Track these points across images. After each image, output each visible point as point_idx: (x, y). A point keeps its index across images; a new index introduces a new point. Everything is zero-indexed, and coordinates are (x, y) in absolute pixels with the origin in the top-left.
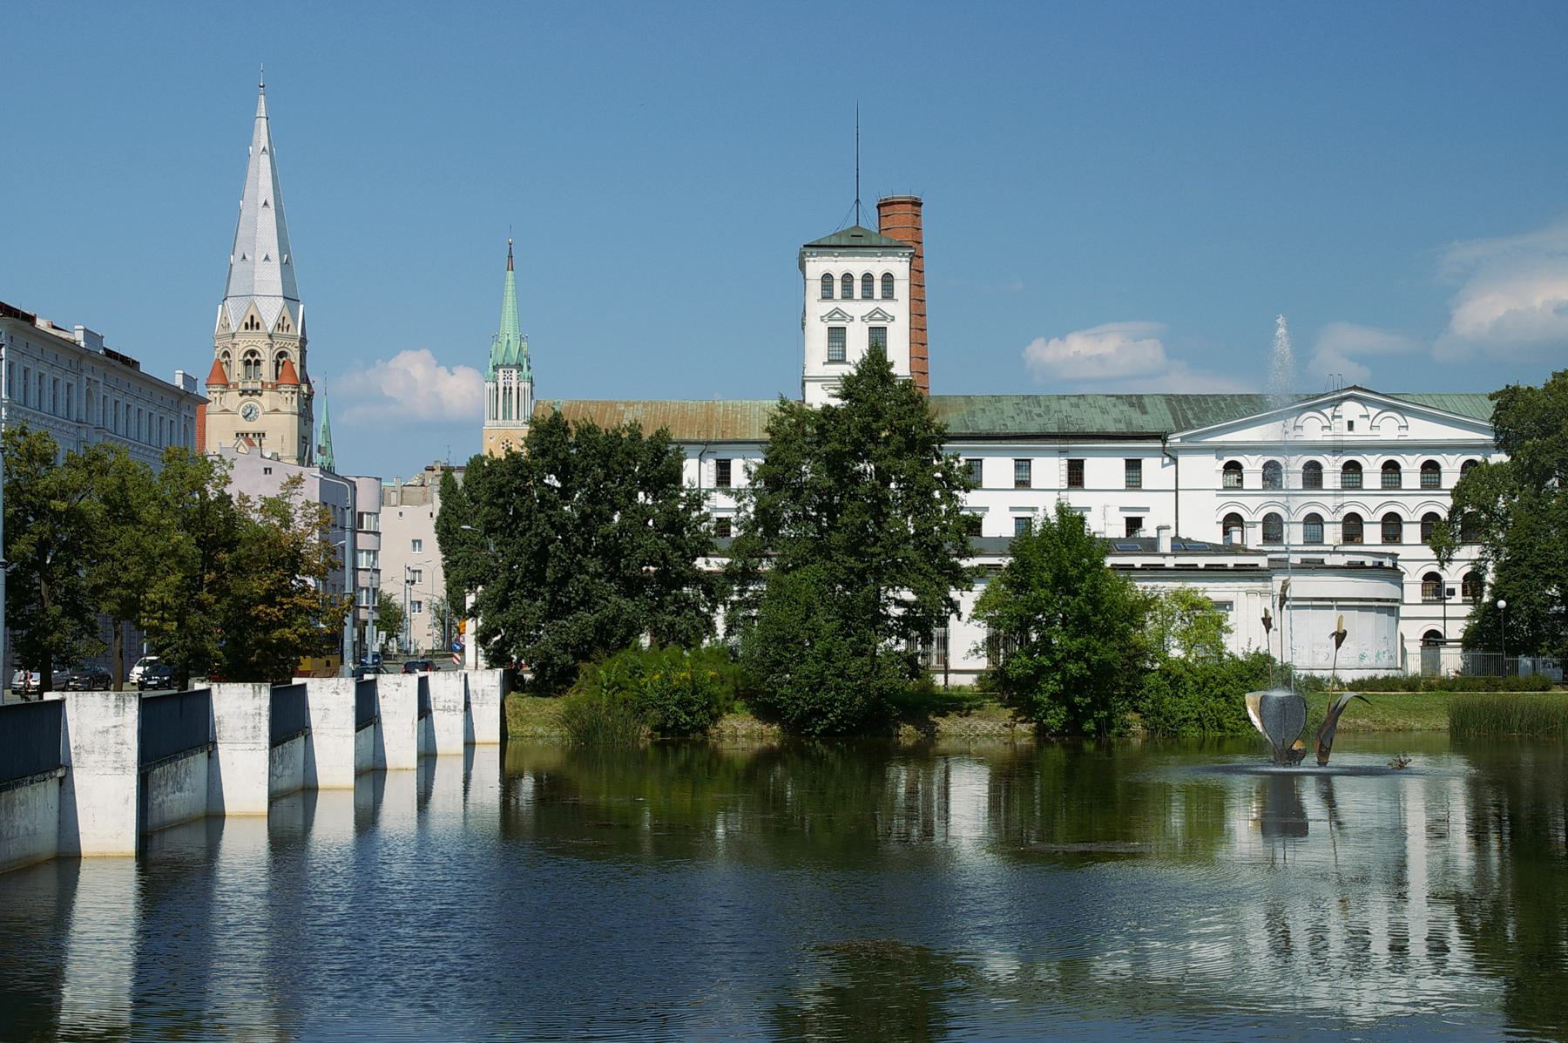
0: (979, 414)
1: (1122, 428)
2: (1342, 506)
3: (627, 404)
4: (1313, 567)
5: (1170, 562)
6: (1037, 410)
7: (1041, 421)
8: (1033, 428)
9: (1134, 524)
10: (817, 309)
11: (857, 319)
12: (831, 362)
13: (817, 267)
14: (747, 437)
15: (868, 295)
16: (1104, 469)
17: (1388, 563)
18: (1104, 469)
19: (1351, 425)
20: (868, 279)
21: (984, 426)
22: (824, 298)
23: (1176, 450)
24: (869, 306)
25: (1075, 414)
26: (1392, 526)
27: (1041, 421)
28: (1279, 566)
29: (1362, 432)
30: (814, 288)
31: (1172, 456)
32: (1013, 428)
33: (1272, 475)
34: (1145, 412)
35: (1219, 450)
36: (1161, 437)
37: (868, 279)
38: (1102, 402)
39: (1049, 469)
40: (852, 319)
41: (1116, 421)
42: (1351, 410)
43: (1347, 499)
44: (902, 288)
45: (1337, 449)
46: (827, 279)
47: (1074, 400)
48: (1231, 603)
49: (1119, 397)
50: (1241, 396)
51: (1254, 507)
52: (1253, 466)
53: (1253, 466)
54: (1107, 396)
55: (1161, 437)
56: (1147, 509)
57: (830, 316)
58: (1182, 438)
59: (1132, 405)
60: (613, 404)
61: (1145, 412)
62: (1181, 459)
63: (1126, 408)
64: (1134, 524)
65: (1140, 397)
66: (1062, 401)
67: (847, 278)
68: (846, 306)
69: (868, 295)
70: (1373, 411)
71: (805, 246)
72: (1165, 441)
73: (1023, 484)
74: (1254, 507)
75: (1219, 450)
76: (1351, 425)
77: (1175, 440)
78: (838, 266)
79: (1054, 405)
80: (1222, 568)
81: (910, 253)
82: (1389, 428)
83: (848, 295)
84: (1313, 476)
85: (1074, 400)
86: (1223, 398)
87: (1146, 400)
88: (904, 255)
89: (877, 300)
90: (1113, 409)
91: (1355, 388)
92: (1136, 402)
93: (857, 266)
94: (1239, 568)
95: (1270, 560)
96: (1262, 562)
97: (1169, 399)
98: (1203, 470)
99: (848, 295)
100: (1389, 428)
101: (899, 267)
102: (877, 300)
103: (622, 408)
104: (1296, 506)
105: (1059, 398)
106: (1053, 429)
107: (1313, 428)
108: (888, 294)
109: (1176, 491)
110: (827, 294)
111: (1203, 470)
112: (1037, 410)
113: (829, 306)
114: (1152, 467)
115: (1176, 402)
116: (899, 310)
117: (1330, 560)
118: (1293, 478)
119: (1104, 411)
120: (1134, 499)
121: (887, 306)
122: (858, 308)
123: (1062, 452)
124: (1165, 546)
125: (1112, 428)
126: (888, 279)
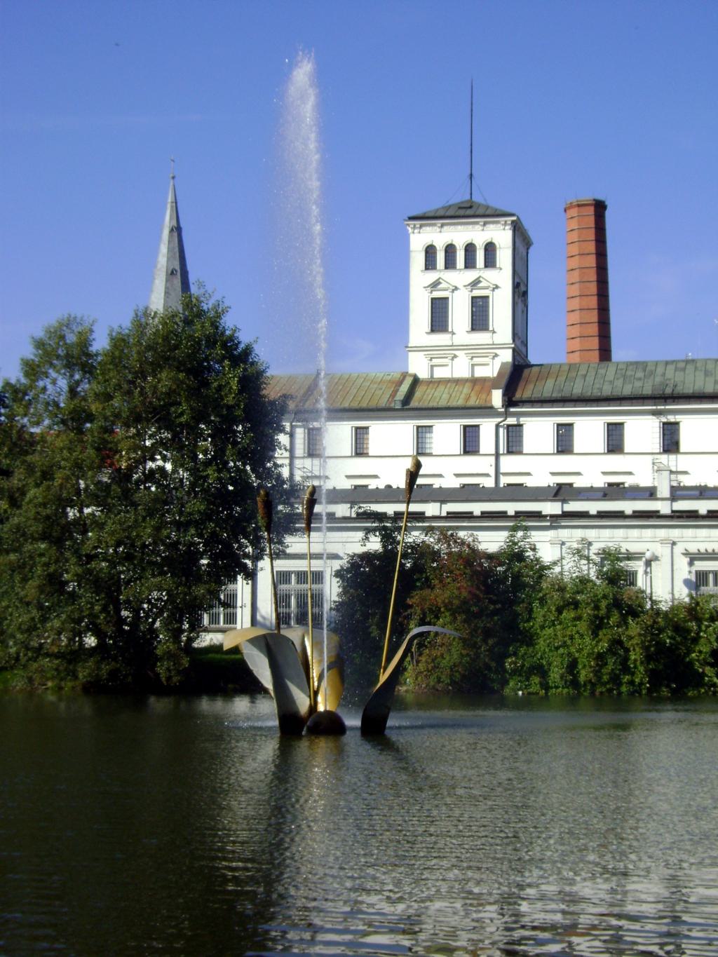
5: (664, 508)
8: (627, 391)
10: (419, 279)
13: (420, 239)
15: (470, 263)
20: (470, 249)
22: (427, 268)
24: (471, 275)
25: (679, 377)
27: (638, 384)
30: (418, 260)
32: (607, 391)
37: (470, 249)
40: (456, 288)
44: (505, 257)
46: (430, 251)
57: (435, 285)
66: (671, 368)
67: (450, 250)
68: (452, 277)
69: (470, 263)
78: (439, 236)
81: (513, 222)
83: (450, 264)
85: (682, 365)
88: (506, 224)
89: (480, 269)
93: (460, 235)
99: (450, 264)
101: (502, 236)
102: (480, 269)
105: (667, 363)
106: (648, 390)
108: (490, 262)
110: (430, 264)
113: (432, 276)
116: (502, 276)
121: (490, 276)
122: (460, 277)
124: (664, 491)
126: (490, 249)
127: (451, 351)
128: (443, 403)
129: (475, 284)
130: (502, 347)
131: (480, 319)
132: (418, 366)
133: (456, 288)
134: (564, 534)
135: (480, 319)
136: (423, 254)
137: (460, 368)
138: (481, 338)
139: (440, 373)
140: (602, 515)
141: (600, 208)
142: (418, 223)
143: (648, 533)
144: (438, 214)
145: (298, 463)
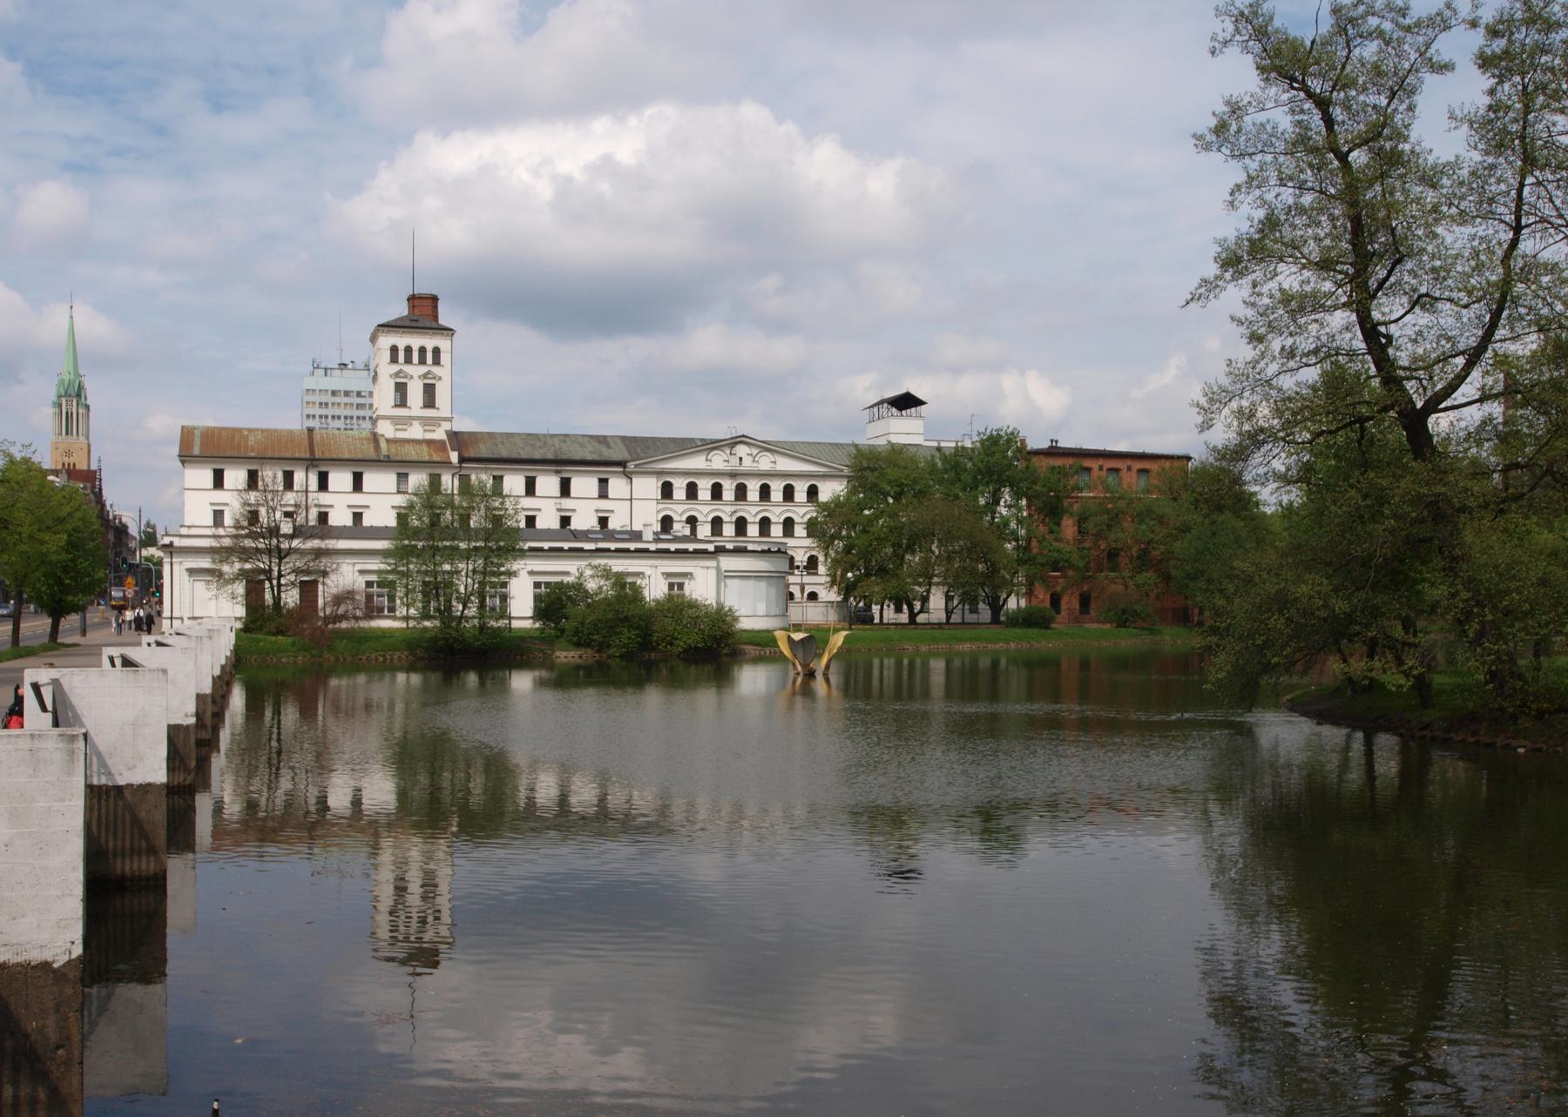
0: (500, 446)
1: (595, 457)
2: (735, 512)
3: (250, 430)
4: (740, 551)
5: (652, 547)
6: (539, 444)
7: (541, 451)
8: (537, 456)
9: (603, 521)
11: (415, 376)
12: (396, 406)
13: (386, 341)
14: (340, 456)
15: (422, 361)
16: (585, 485)
17: (783, 550)
18: (585, 485)
19: (741, 459)
21: (504, 454)
23: (632, 473)
24: (423, 369)
26: (789, 525)
28: (720, 550)
29: (747, 462)
31: (628, 476)
32: (524, 455)
33: (692, 491)
34: (608, 446)
35: (659, 473)
36: (622, 464)
38: (581, 440)
39: (548, 484)
41: (591, 452)
42: (742, 450)
43: (738, 507)
45: (733, 475)
46: (394, 349)
47: (562, 438)
48: (691, 574)
49: (591, 437)
50: (669, 439)
51: (679, 510)
52: (679, 486)
53: (679, 486)
54: (583, 436)
55: (622, 464)
56: (612, 511)
57: (397, 375)
58: (636, 466)
59: (600, 442)
60: (239, 430)
61: (608, 446)
62: (635, 480)
63: (595, 444)
64: (603, 521)
65: (605, 437)
66: (555, 439)
68: (408, 369)
69: (422, 361)
70: (755, 451)
71: (379, 326)
72: (625, 467)
73: (603, 495)
74: (679, 510)
75: (659, 473)
76: (741, 459)
77: (631, 466)
78: (402, 341)
79: (549, 440)
80: (685, 551)
82: (765, 463)
83: (408, 360)
84: (717, 492)
85: (562, 438)
86: (659, 439)
87: (609, 439)
90: (588, 445)
91: (743, 436)
92: (602, 440)
93: (416, 341)
94: (696, 552)
95: (716, 547)
96: (711, 548)
97: (624, 439)
98: (648, 487)
100: (765, 463)
103: (246, 433)
104: (705, 511)
106: (550, 456)
107: (718, 461)
108: (437, 361)
109: (631, 499)
110: (394, 360)
111: (648, 487)
112: (539, 444)
113: (395, 368)
114: (617, 485)
115: (628, 441)
117: (750, 547)
118: (704, 494)
119: (582, 446)
120: (603, 504)
121: (436, 370)
122: (416, 370)
123: (557, 472)
125: (589, 457)
126: (436, 351)
127: (408, 421)
128: (415, 458)
129: (425, 376)
130: (445, 419)
131: (430, 399)
132: (386, 429)
133: (412, 377)
134: (596, 562)
135: (430, 399)
136: (389, 352)
137: (416, 432)
138: (430, 413)
139: (401, 435)
140: (618, 550)
141: (434, 299)
142: (386, 329)
143: (643, 562)
144: (398, 324)
145: (310, 495)
